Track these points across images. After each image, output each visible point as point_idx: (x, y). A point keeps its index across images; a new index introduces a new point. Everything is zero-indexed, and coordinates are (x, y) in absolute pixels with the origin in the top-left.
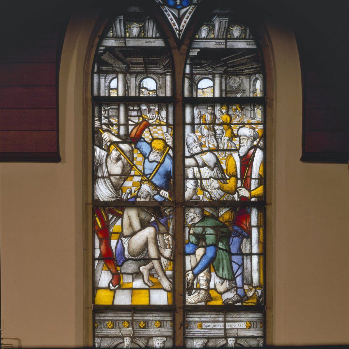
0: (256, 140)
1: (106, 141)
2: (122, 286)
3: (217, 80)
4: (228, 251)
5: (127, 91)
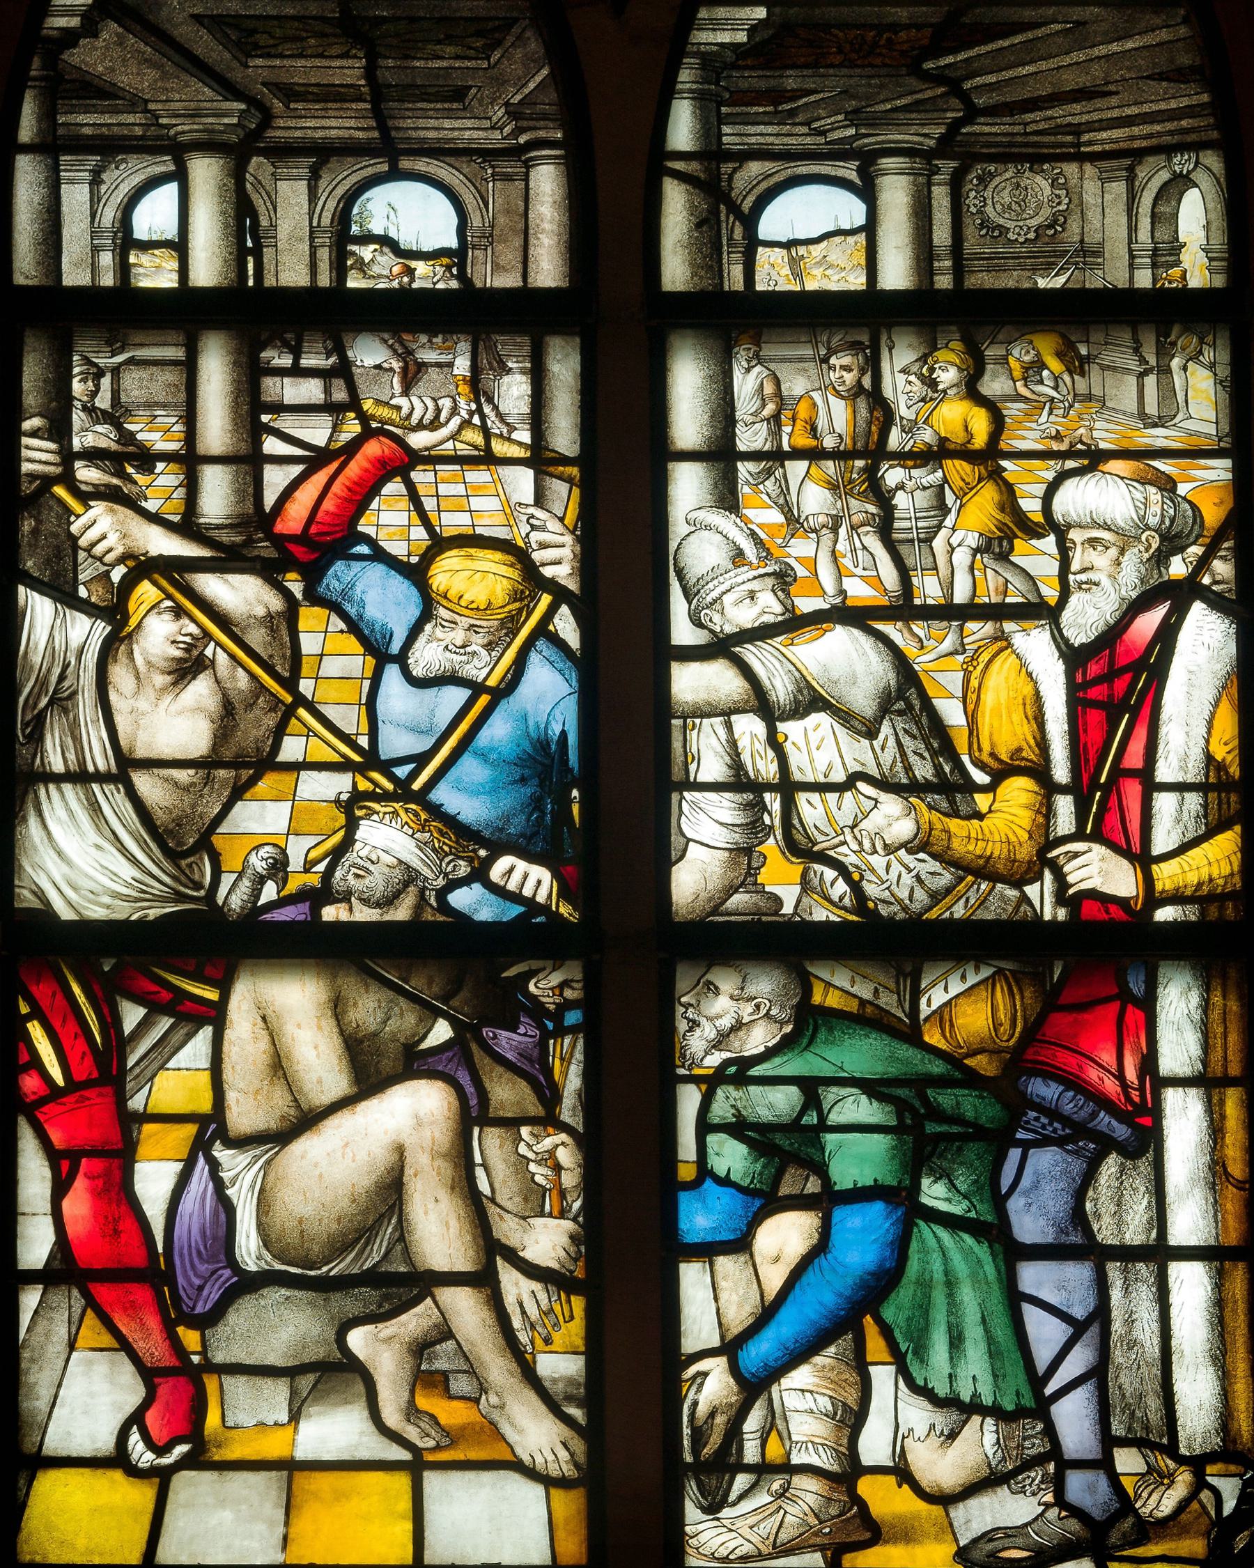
0: (1182, 549)
1: (100, 559)
2: (219, 1446)
5: (250, 260)
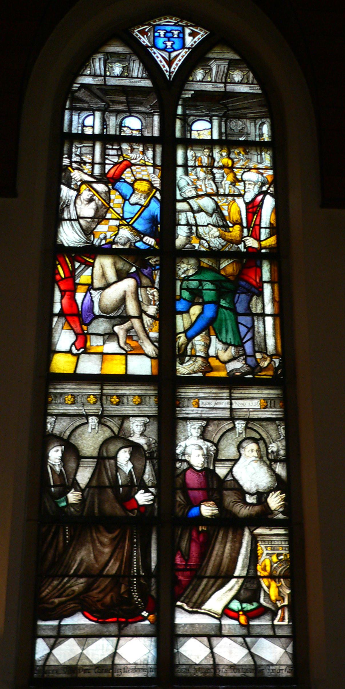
0: (264, 185)
1: (76, 180)
2: (89, 349)
3: (216, 123)
4: (233, 310)
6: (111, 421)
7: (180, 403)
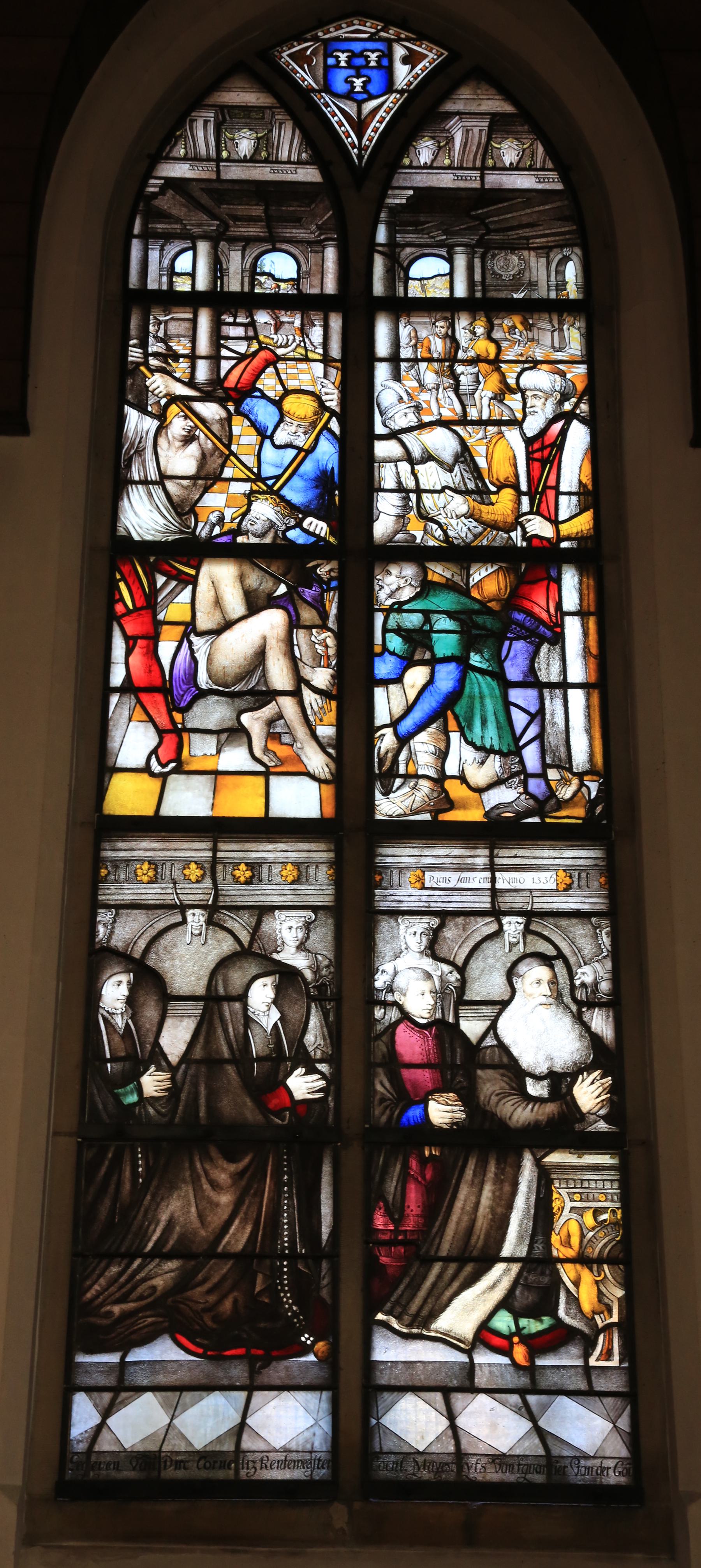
0: (568, 400)
1: (157, 396)
3: (461, 261)
4: (499, 676)
6: (233, 918)
7: (382, 879)
